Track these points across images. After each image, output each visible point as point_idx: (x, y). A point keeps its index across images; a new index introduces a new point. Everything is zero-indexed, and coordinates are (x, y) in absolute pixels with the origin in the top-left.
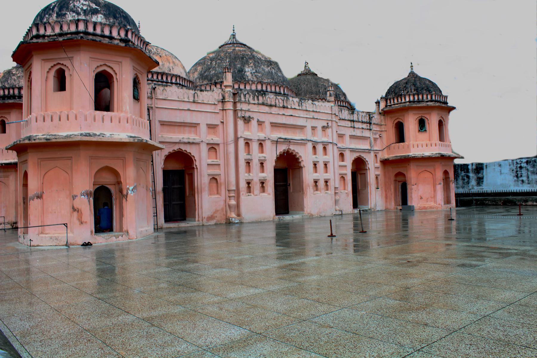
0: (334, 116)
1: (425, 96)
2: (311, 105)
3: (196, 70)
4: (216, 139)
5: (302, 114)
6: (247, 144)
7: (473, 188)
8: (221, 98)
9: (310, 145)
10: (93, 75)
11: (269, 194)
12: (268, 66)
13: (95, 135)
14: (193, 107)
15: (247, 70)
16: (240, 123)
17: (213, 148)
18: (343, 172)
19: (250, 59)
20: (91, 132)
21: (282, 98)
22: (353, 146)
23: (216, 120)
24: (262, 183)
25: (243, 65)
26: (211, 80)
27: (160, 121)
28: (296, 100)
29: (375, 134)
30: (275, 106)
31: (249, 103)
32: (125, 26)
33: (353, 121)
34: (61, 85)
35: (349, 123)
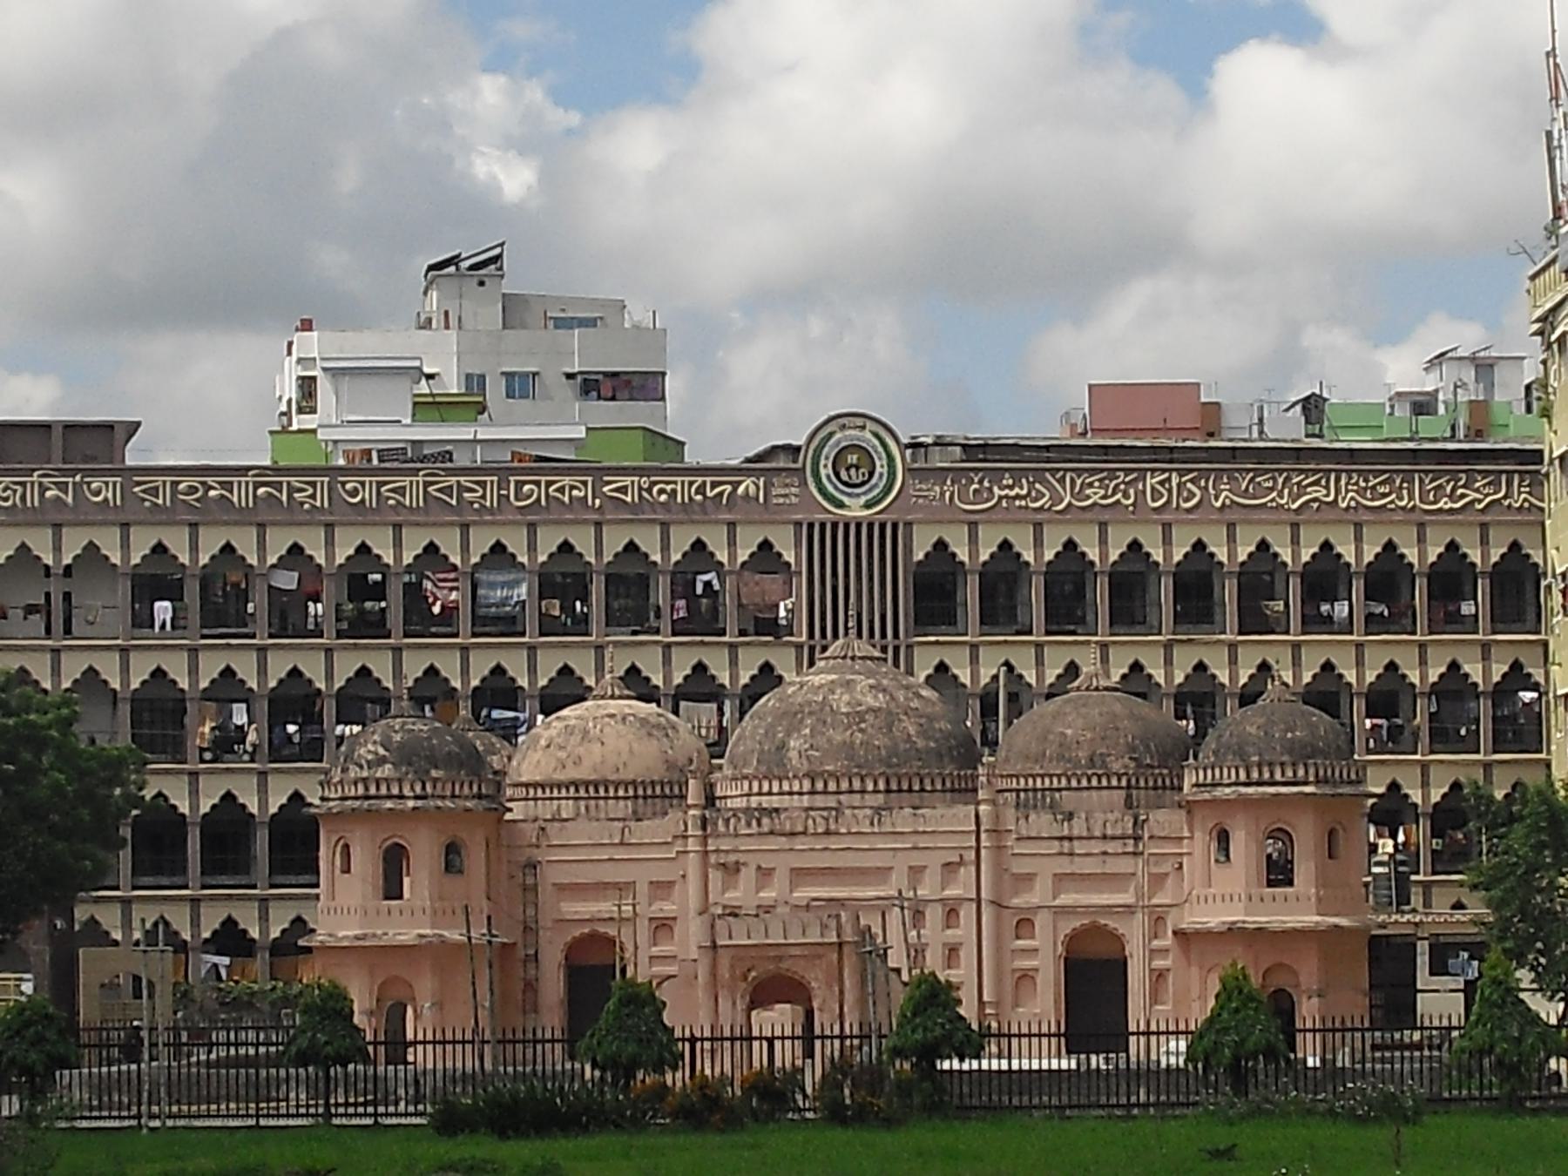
2: (911, 819)
4: (668, 908)
10: (380, 853)
13: (374, 935)
15: (792, 743)
16: (715, 876)
19: (811, 713)
21: (825, 814)
22: (1064, 899)
25: (789, 735)
29: (1156, 864)
30: (804, 833)
31: (737, 836)
32: (428, 772)
33: (1070, 839)
35: (1055, 847)
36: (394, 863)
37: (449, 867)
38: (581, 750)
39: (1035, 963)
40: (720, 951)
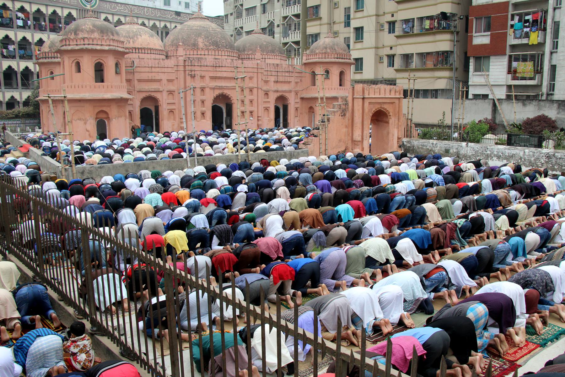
9: (238, 89)
10: (94, 65)
16: (188, 78)
18: (267, 105)
23: (173, 77)
34: (79, 70)
36: (99, 70)
39: (268, 106)
40: (365, 100)
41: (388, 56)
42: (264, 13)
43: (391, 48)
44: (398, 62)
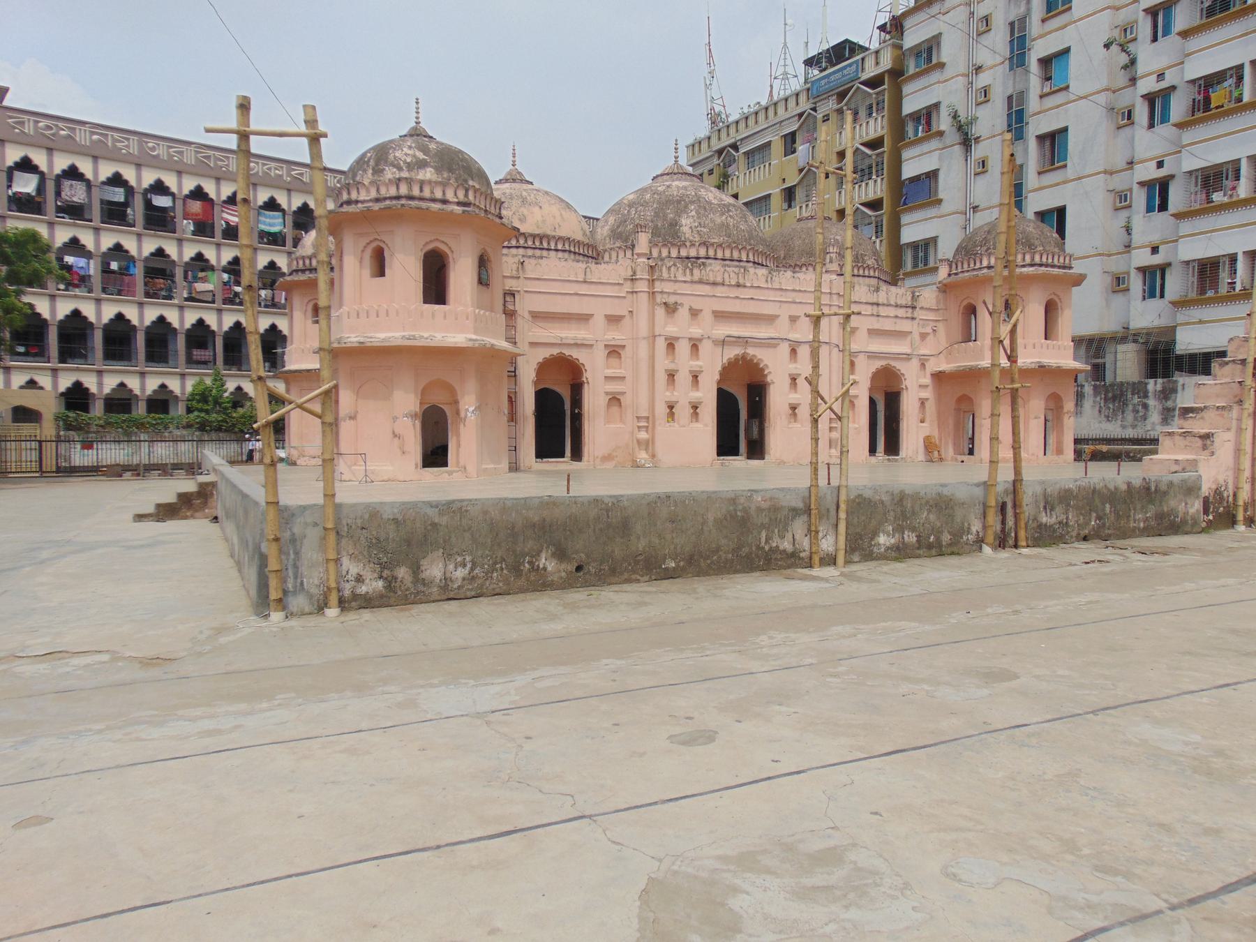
0: (835, 297)
1: (1020, 257)
3: (607, 222)
5: (772, 296)
6: (671, 346)
7: (1153, 429)
8: (630, 273)
9: (785, 348)
11: (706, 425)
12: (723, 214)
14: (584, 289)
15: (684, 222)
16: (660, 312)
17: (614, 351)
19: (692, 202)
20: (417, 334)
21: (736, 270)
24: (695, 407)
25: (679, 214)
26: (626, 240)
27: (530, 312)
28: (762, 272)
31: (676, 281)
32: (466, 181)
33: (878, 305)
34: (380, 270)
37: (480, 282)
38: (524, 211)
41: (1143, 270)
42: (790, 206)
43: (1155, 250)
44: (1175, 285)
